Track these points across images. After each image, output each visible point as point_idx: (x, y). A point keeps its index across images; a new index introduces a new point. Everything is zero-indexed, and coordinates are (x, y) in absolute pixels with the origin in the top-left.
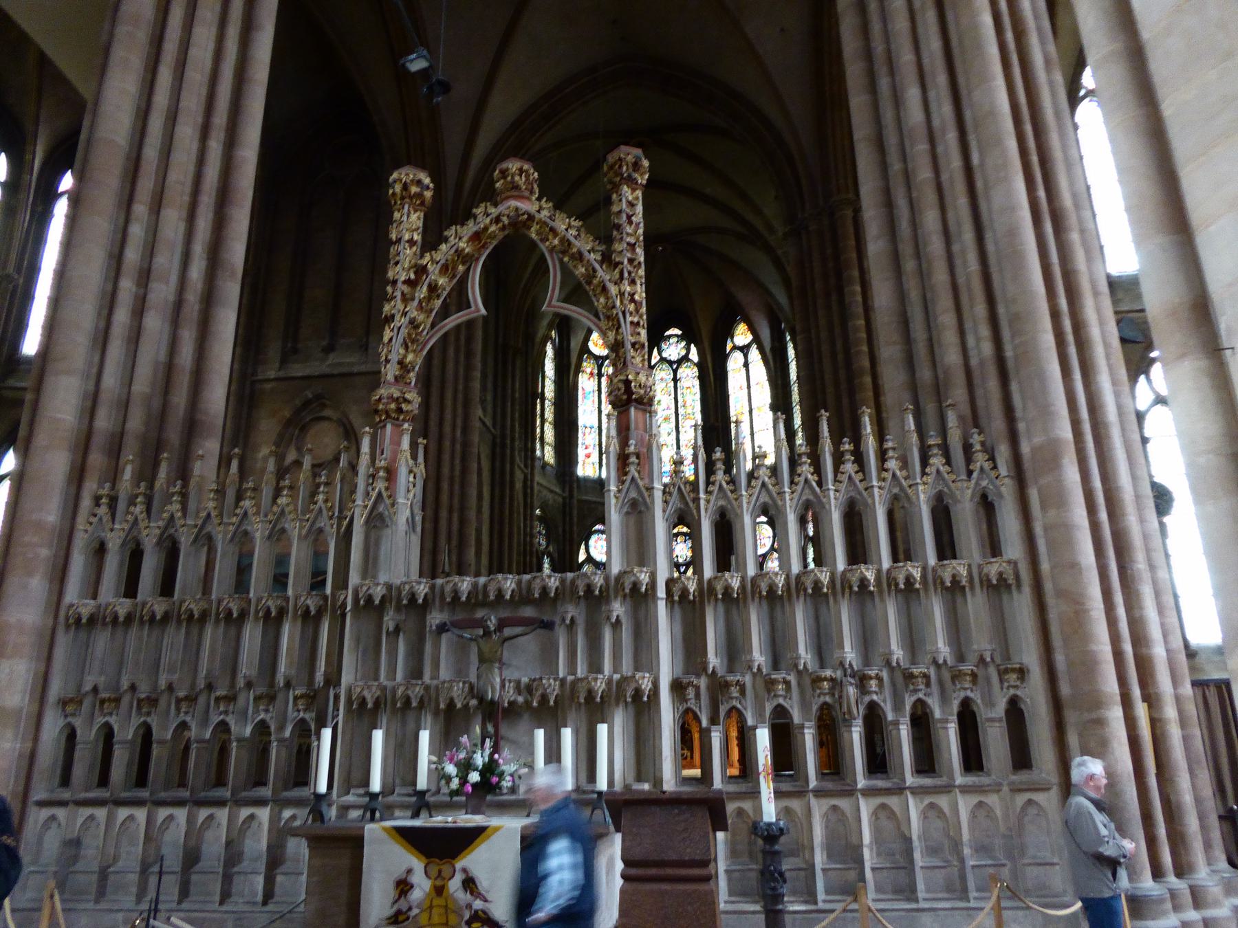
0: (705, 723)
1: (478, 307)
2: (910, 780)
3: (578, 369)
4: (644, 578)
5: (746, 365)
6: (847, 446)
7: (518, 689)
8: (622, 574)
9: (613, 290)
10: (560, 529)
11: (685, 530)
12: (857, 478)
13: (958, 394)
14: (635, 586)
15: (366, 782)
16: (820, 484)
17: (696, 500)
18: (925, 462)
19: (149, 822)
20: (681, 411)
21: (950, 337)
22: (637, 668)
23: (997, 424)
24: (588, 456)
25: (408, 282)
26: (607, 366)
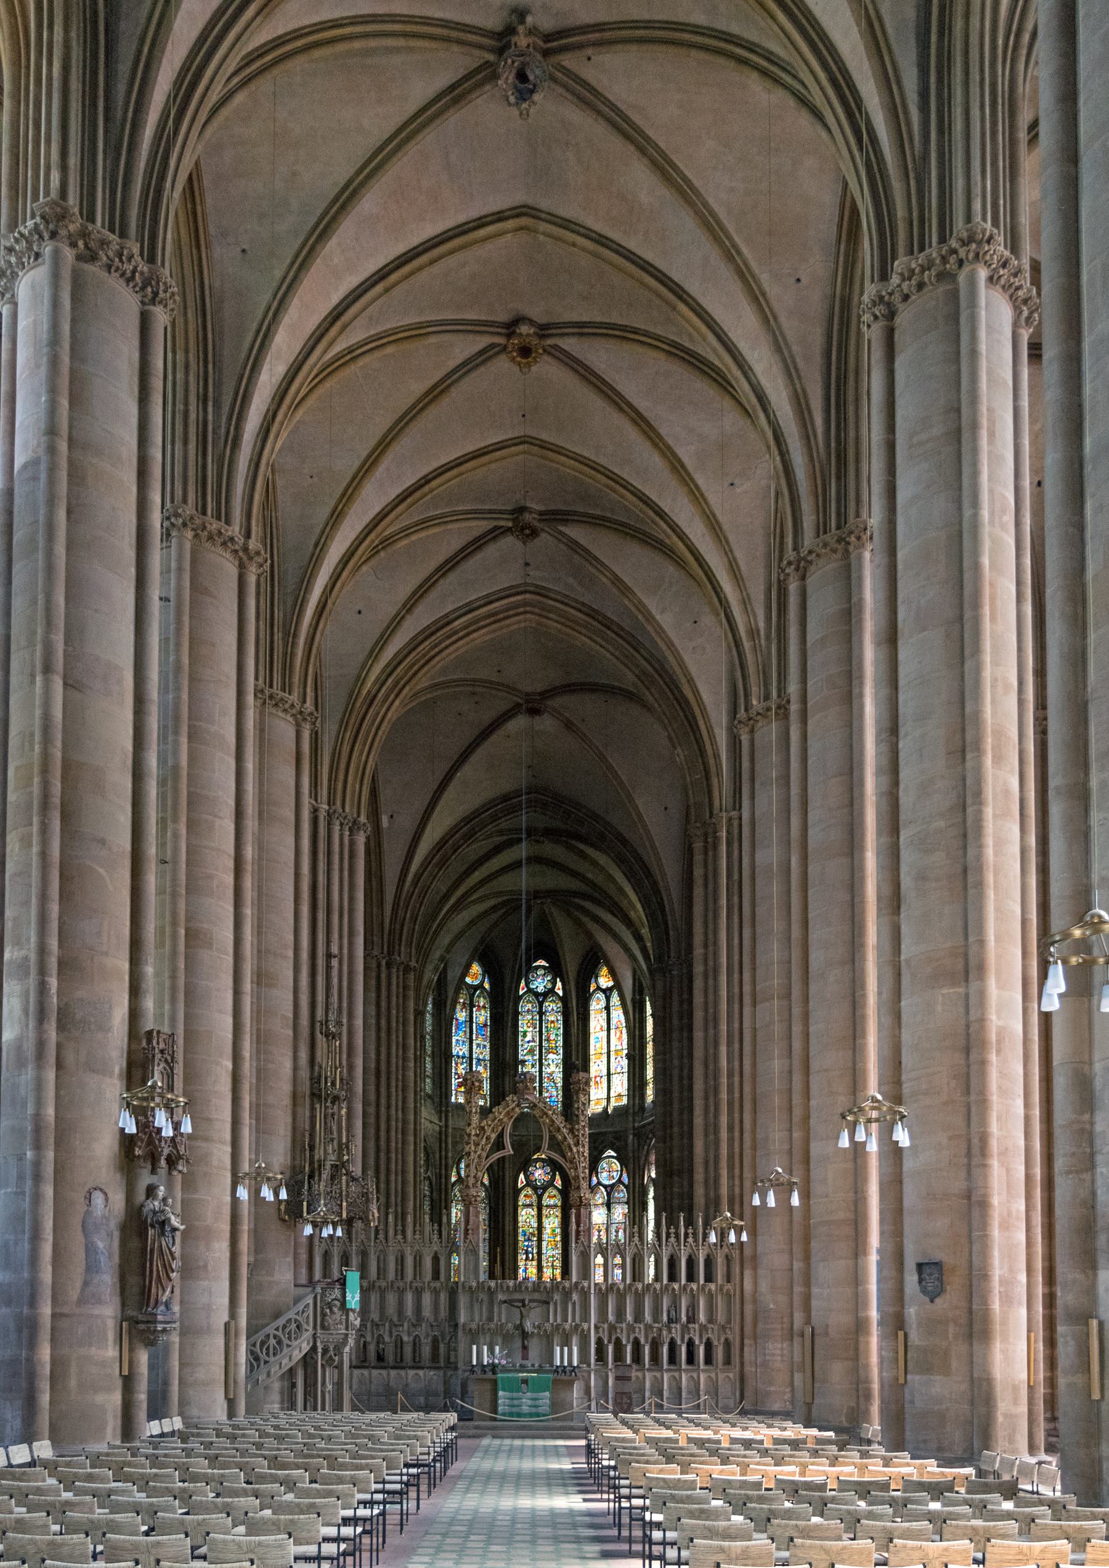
1: (509, 1150)
3: (455, 1002)
4: (586, 1284)
7: (534, 1327)
8: (576, 1283)
10: (437, 1156)
15: (471, 1361)
22: (581, 1321)
25: (477, 1135)
26: (479, 996)
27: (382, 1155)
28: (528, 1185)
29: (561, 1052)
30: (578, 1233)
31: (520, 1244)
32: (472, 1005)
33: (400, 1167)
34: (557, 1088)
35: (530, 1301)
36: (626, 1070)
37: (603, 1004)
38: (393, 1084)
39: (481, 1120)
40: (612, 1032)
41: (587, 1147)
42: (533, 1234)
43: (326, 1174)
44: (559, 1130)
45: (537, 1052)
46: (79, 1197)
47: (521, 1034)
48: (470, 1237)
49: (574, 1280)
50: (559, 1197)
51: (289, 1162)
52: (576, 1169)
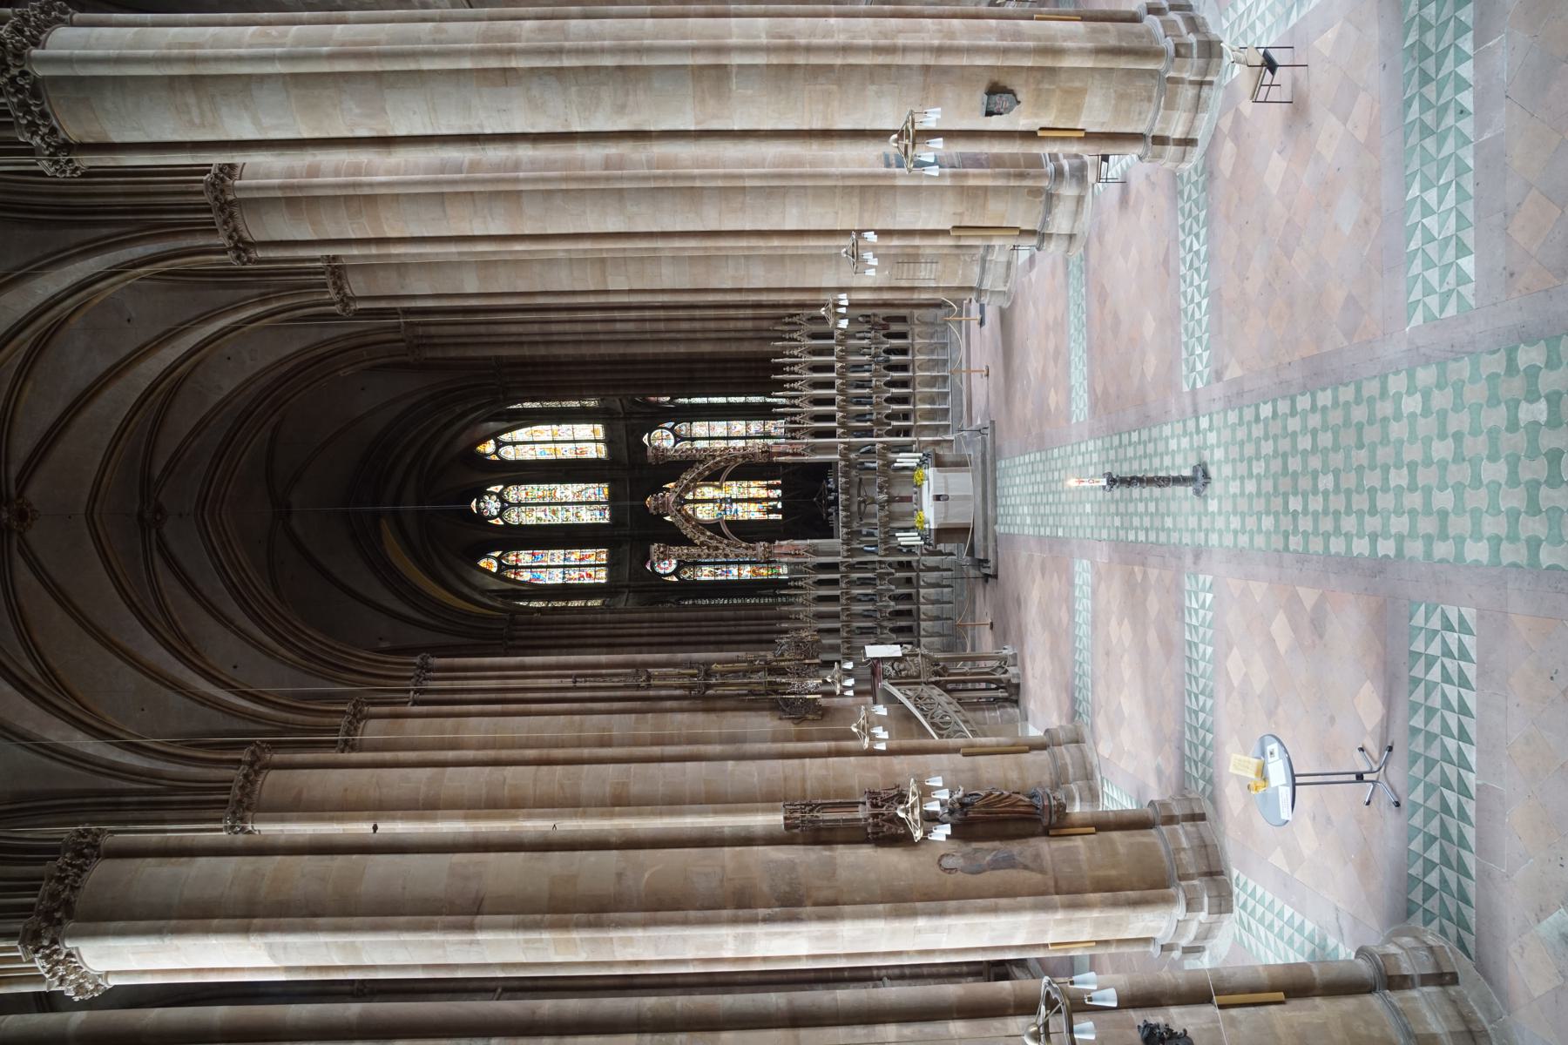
2: (910, 357)
3: (515, 581)
4: (842, 446)
6: (788, 369)
9: (718, 459)
12: (800, 366)
13: (765, 324)
14: (845, 449)
17: (807, 428)
18: (796, 340)
19: (926, 637)
20: (547, 500)
21: (740, 325)
23: (782, 312)
24: (589, 576)
25: (708, 548)
27: (685, 639)
29: (553, 486)
30: (794, 454)
32: (516, 567)
33: (694, 624)
34: (586, 488)
35: (859, 495)
36: (570, 426)
37: (510, 448)
38: (620, 632)
39: (696, 545)
44: (700, 474)
45: (555, 508)
46: (950, 879)
47: (539, 522)
48: (801, 552)
49: (838, 457)
51: (768, 713)
52: (736, 457)
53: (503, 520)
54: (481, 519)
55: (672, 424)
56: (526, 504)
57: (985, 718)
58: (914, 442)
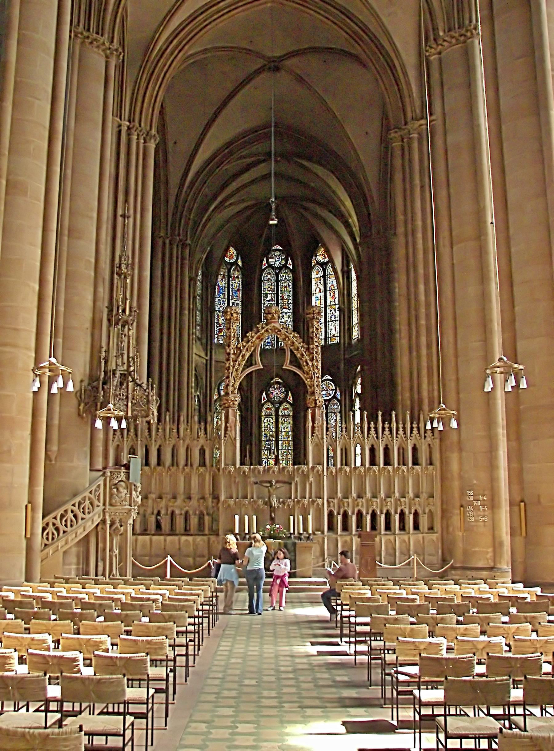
0: (336, 514)
5: (324, 277)
6: (387, 425)
7: (279, 502)
9: (310, 364)
11: (280, 380)
16: (377, 437)
18: (411, 432)
21: (425, 386)
24: (220, 331)
26: (234, 270)
28: (268, 401)
29: (291, 307)
30: (313, 427)
31: (263, 443)
32: (229, 276)
35: (277, 482)
37: (321, 274)
40: (328, 293)
41: (320, 362)
42: (272, 436)
43: (116, 381)
50: (291, 409)
52: (311, 378)
53: (265, 269)
54: (267, 253)
55: (339, 397)
56: (277, 286)
57: (70, 564)
58: (323, 533)
